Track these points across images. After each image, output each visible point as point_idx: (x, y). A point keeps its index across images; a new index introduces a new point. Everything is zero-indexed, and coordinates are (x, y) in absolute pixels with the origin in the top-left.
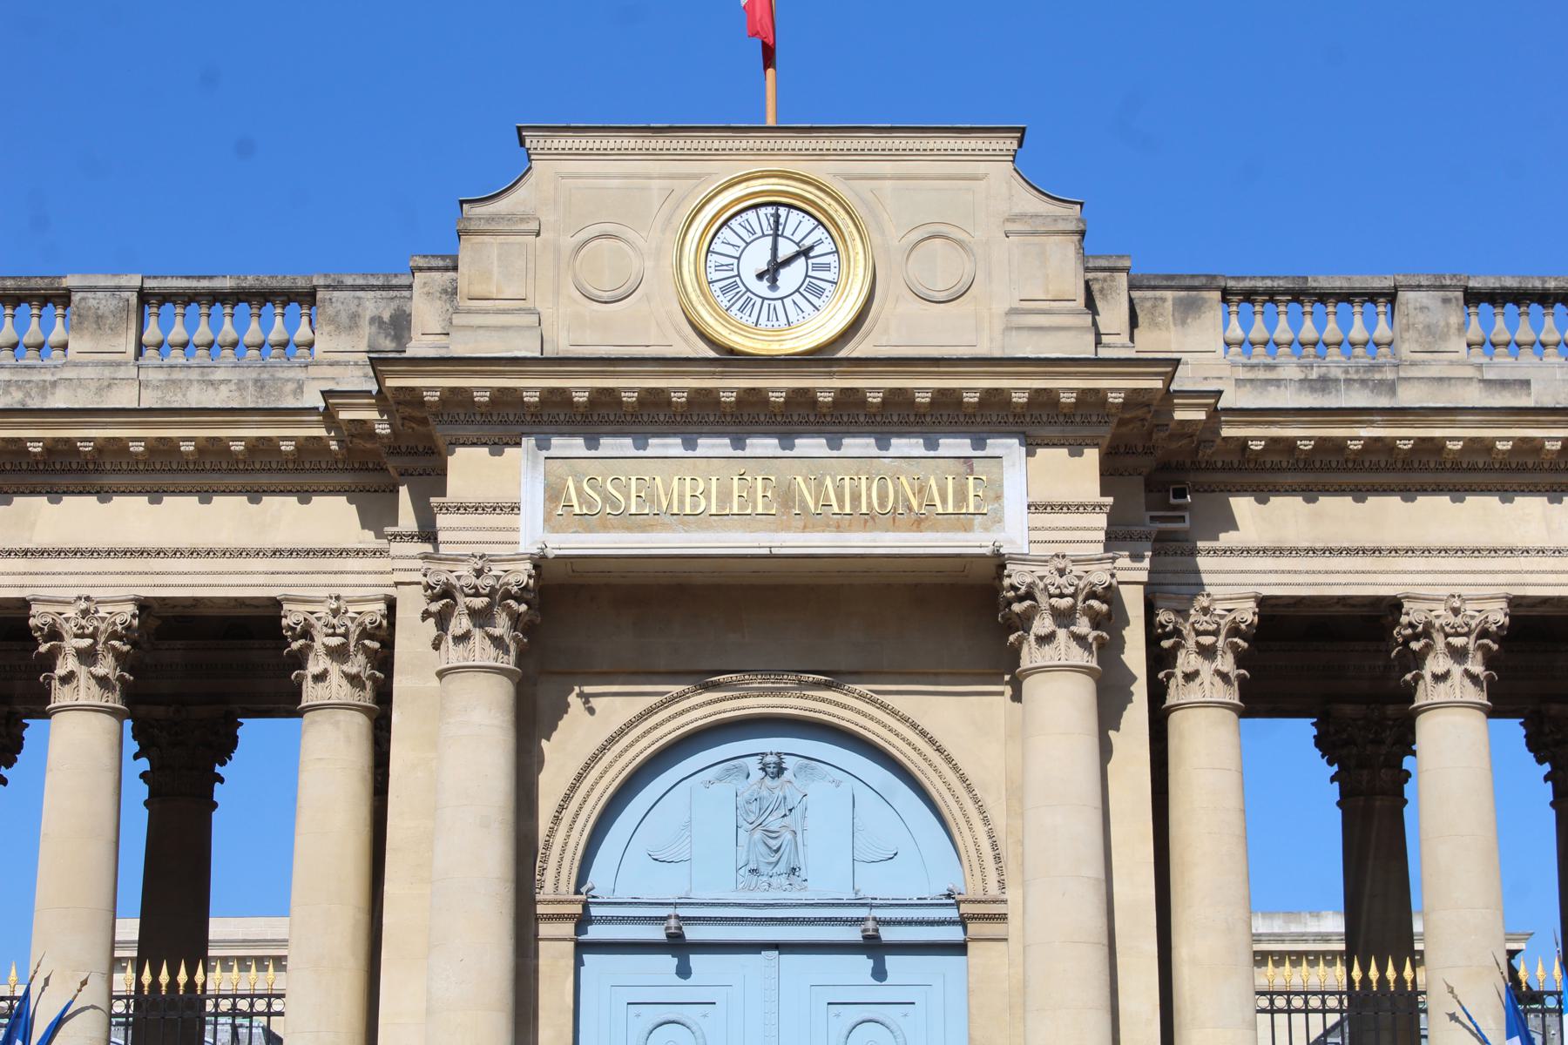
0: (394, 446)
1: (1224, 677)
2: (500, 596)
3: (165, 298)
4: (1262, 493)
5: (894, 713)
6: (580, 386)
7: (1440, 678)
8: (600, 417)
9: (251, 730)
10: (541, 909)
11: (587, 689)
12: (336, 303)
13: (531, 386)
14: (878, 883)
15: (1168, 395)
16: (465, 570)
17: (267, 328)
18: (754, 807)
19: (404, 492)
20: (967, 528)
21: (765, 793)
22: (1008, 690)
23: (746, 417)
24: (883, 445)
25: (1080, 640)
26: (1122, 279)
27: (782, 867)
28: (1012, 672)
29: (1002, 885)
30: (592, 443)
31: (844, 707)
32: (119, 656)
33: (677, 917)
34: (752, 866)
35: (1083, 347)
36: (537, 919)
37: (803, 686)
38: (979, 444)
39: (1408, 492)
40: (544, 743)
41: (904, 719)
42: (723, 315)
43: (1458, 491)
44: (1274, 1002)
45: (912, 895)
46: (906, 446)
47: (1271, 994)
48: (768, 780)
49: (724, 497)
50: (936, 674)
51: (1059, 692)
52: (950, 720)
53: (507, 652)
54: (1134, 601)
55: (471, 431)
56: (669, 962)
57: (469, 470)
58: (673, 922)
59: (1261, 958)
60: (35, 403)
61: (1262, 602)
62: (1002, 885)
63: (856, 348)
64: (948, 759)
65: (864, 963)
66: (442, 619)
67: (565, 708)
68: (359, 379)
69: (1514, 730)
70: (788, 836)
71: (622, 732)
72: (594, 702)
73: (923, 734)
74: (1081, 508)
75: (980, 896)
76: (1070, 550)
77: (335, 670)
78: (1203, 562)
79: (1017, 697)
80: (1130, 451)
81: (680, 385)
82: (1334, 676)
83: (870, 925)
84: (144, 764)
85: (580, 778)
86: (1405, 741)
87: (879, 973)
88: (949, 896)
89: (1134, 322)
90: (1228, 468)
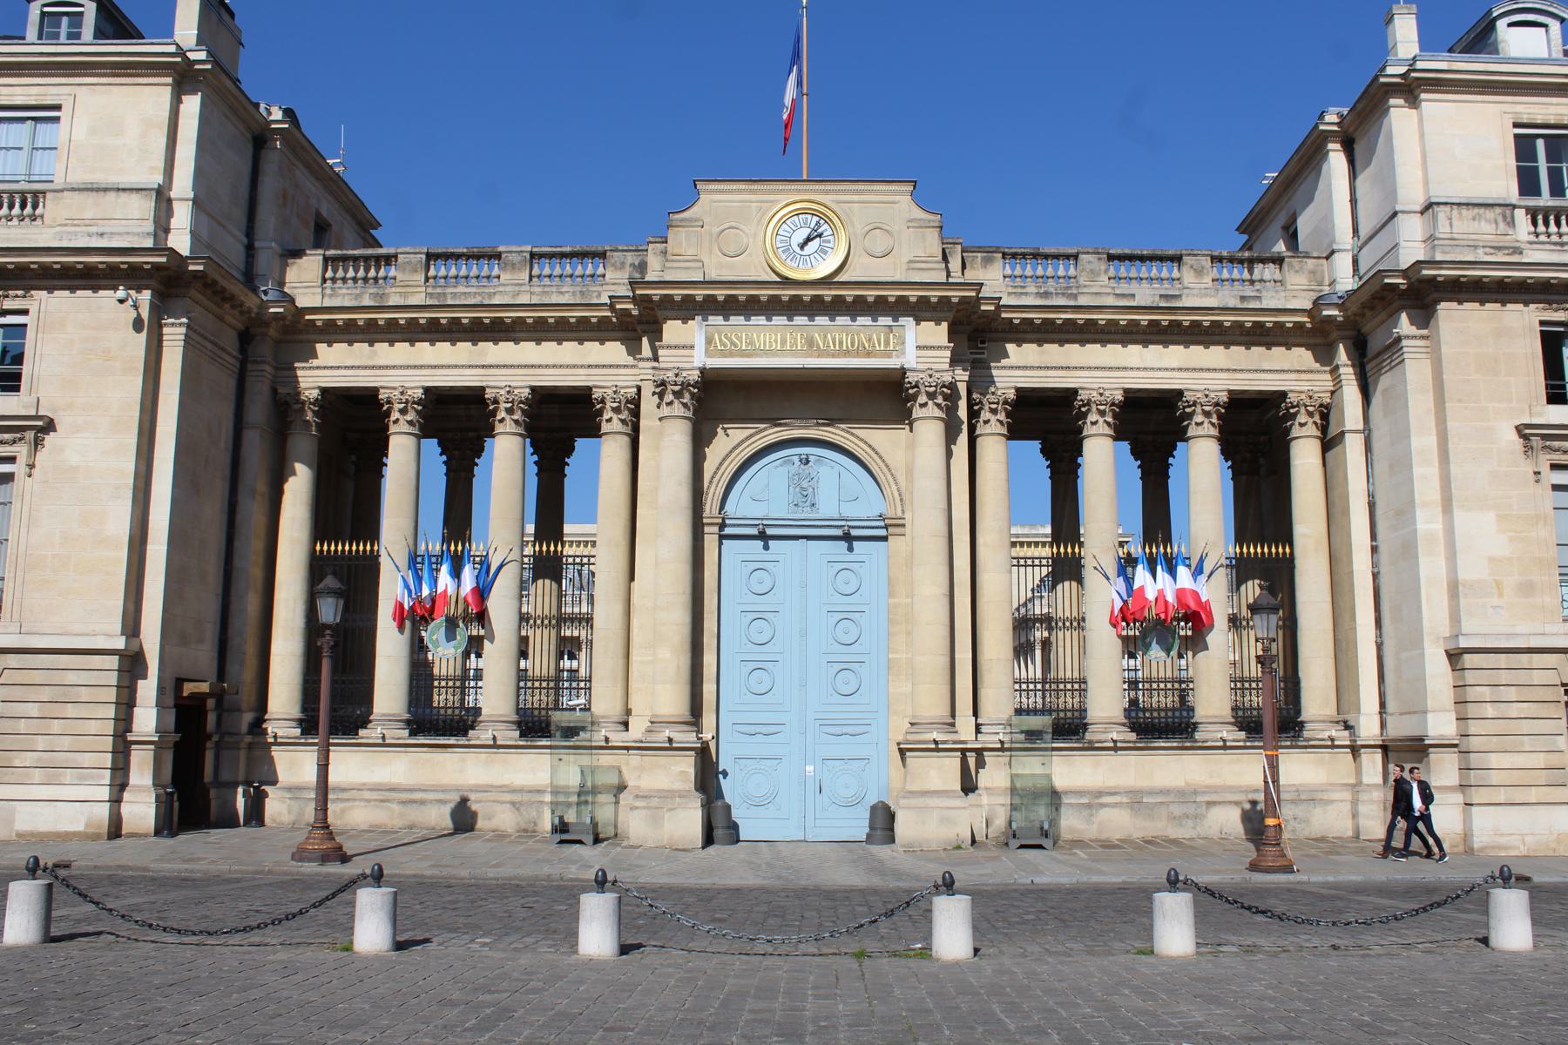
0: (640, 320)
1: (1001, 422)
2: (685, 385)
3: (542, 256)
4: (1019, 342)
6: (721, 294)
7: (1094, 423)
8: (729, 307)
9: (580, 443)
12: (616, 257)
13: (700, 293)
14: (850, 511)
15: (978, 299)
16: (670, 374)
17: (585, 269)
19: (645, 340)
20: (889, 356)
23: (793, 307)
24: (854, 320)
25: (938, 405)
26: (959, 248)
30: (727, 319)
32: (523, 411)
35: (941, 277)
37: (819, 425)
38: (896, 320)
39: (1082, 342)
42: (783, 264)
43: (1104, 343)
44: (1019, 563)
46: (863, 320)
47: (1018, 558)
49: (784, 342)
51: (928, 427)
52: (881, 440)
54: (962, 388)
55: (670, 313)
56: (760, 544)
57: (673, 330)
59: (1014, 544)
60: (486, 302)
61: (1018, 390)
63: (842, 278)
65: (844, 545)
66: (661, 395)
68: (624, 291)
69: (1125, 446)
71: (739, 445)
74: (939, 348)
76: (935, 367)
77: (615, 417)
78: (994, 372)
80: (961, 323)
81: (764, 293)
82: (1049, 421)
84: (535, 458)
86: (1079, 451)
89: (964, 267)
90: (1004, 331)
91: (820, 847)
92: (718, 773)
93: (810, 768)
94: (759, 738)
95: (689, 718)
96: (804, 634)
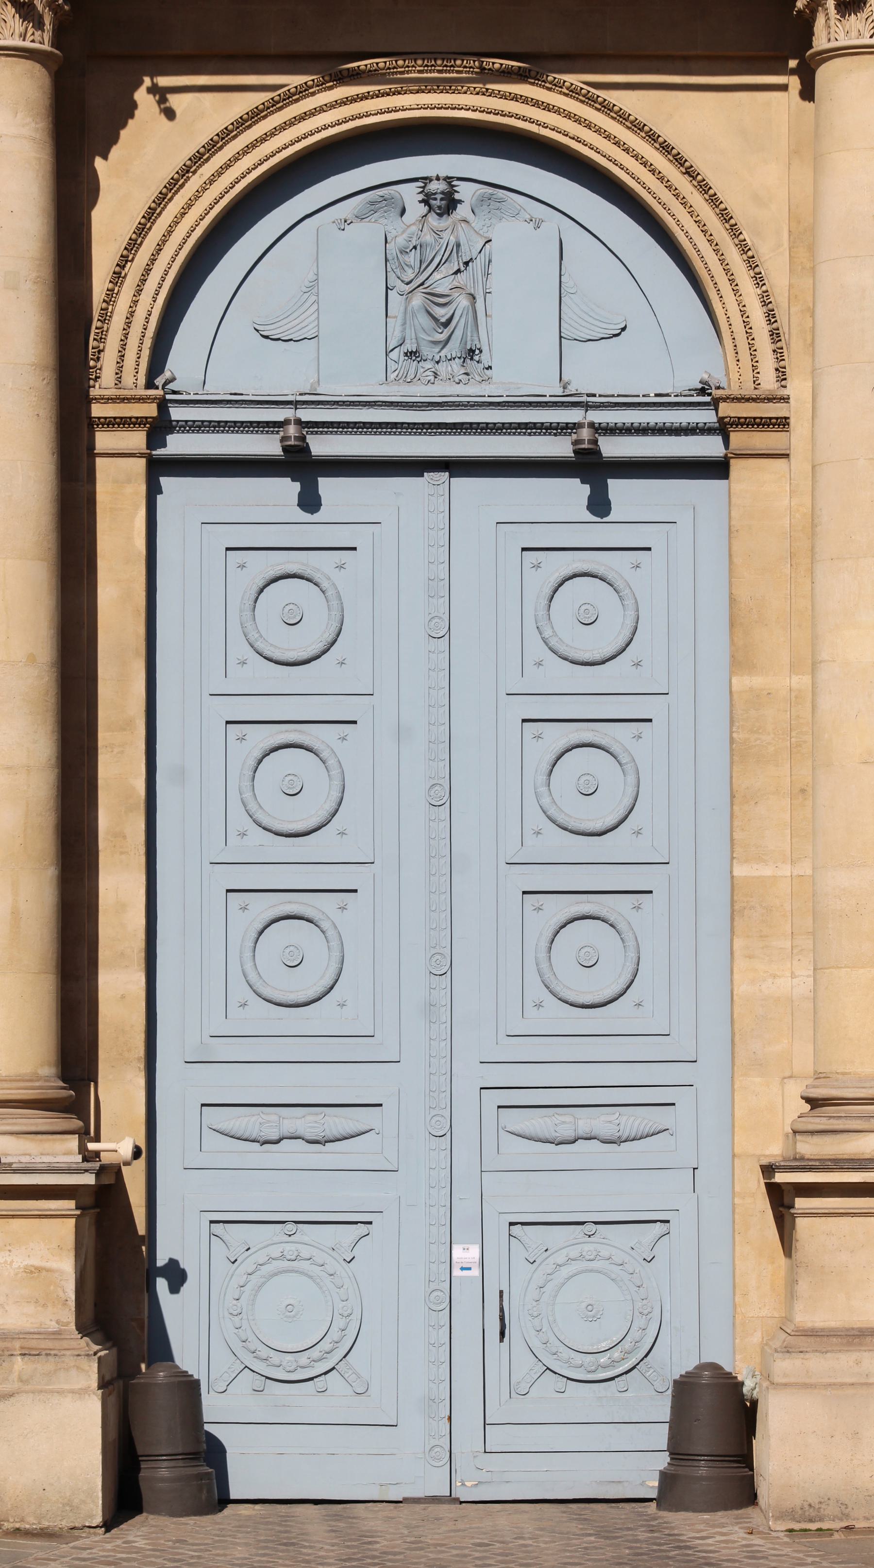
5: (622, 117)
10: (97, 411)
11: (164, 81)
14: (598, 372)
18: (412, 258)
21: (428, 238)
22: (794, 82)
27: (454, 348)
28: (799, 53)
29: (781, 375)
31: (548, 108)
33: (299, 422)
34: (410, 346)
36: (92, 424)
37: (487, 75)
40: (99, 162)
41: (637, 127)
45: (645, 385)
48: (433, 219)
50: (686, 58)
53: (39, 25)
56: (287, 488)
58: (292, 430)
62: (781, 375)
64: (704, 187)
65: (575, 491)
67: (131, 108)
70: (463, 302)
71: (213, 146)
72: (174, 100)
73: (666, 148)
75: (748, 390)
79: (808, 93)
83: (585, 434)
85: (151, 215)
87: (599, 505)
88: (702, 391)
91: (503, 1518)
92: (152, 1272)
93: (466, 1253)
94: (293, 1153)
95: (56, 1089)
96: (443, 799)
